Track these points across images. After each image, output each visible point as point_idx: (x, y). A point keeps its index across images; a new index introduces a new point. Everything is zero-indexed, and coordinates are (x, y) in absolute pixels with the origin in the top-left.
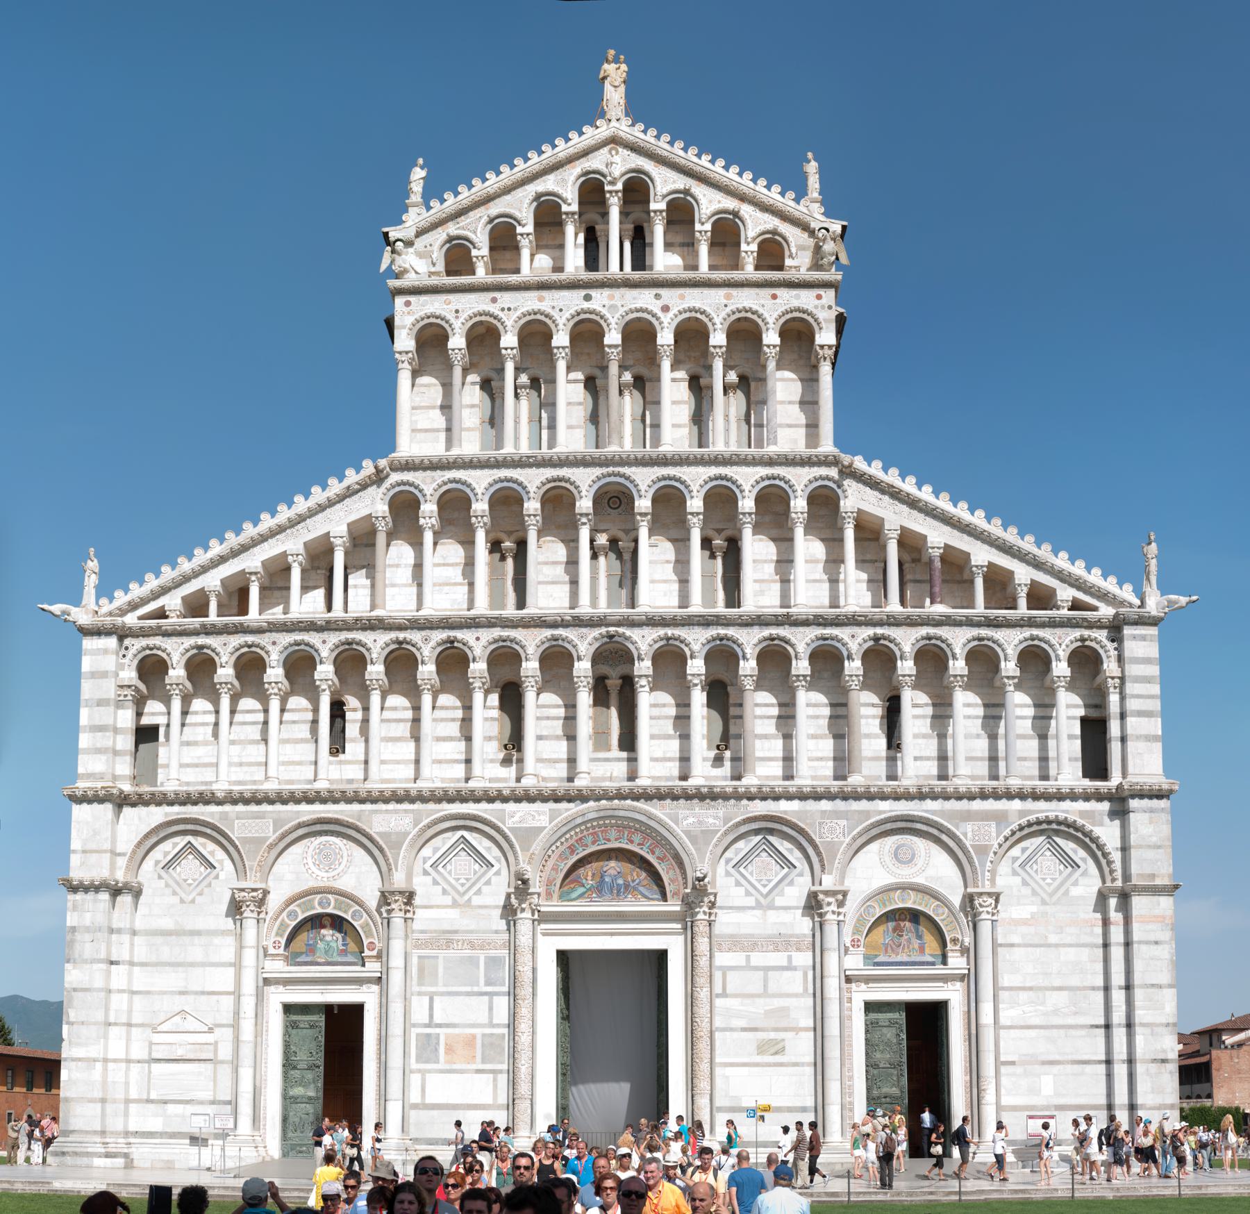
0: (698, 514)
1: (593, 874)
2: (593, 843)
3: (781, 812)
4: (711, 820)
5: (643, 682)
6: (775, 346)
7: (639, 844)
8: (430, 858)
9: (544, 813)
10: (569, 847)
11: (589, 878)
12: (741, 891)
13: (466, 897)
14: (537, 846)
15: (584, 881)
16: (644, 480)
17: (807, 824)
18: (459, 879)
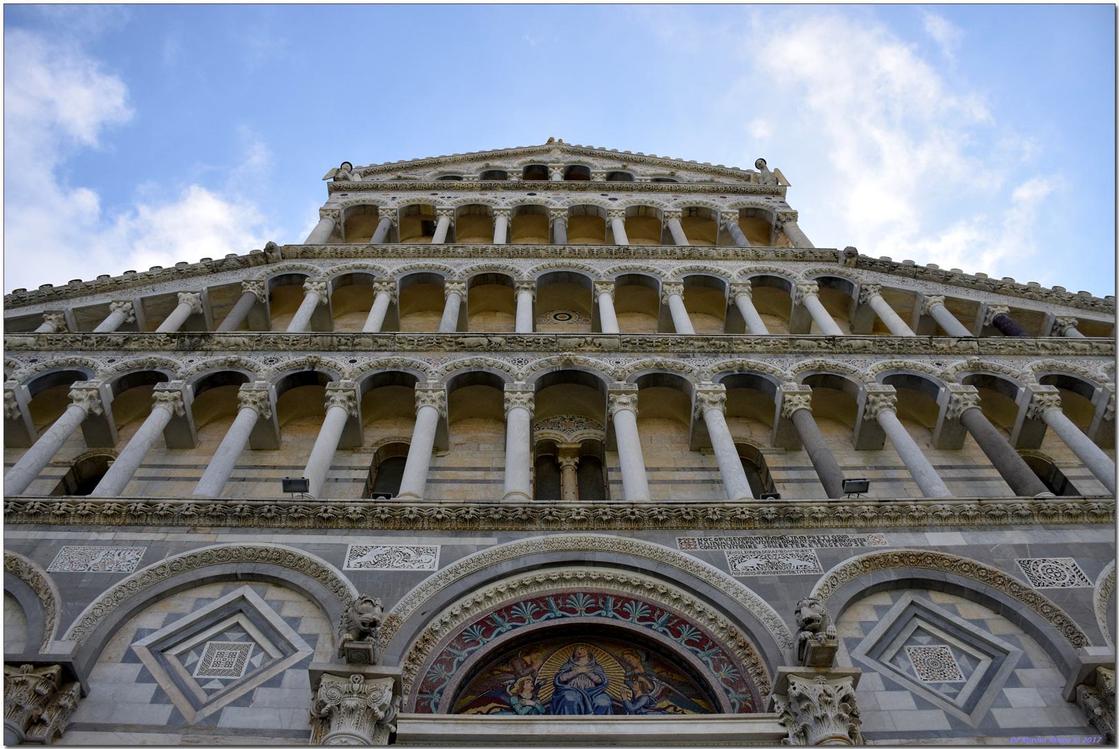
0: (676, 284)
1: (537, 688)
2: (537, 615)
3: (935, 548)
4: (795, 562)
5: (624, 398)
6: (734, 214)
7: (641, 619)
8: (152, 631)
9: (429, 551)
10: (481, 623)
11: (527, 694)
12: (903, 700)
13: (207, 712)
14: (407, 606)
15: (514, 700)
16: (602, 270)
17: (996, 565)
18: (207, 681)
